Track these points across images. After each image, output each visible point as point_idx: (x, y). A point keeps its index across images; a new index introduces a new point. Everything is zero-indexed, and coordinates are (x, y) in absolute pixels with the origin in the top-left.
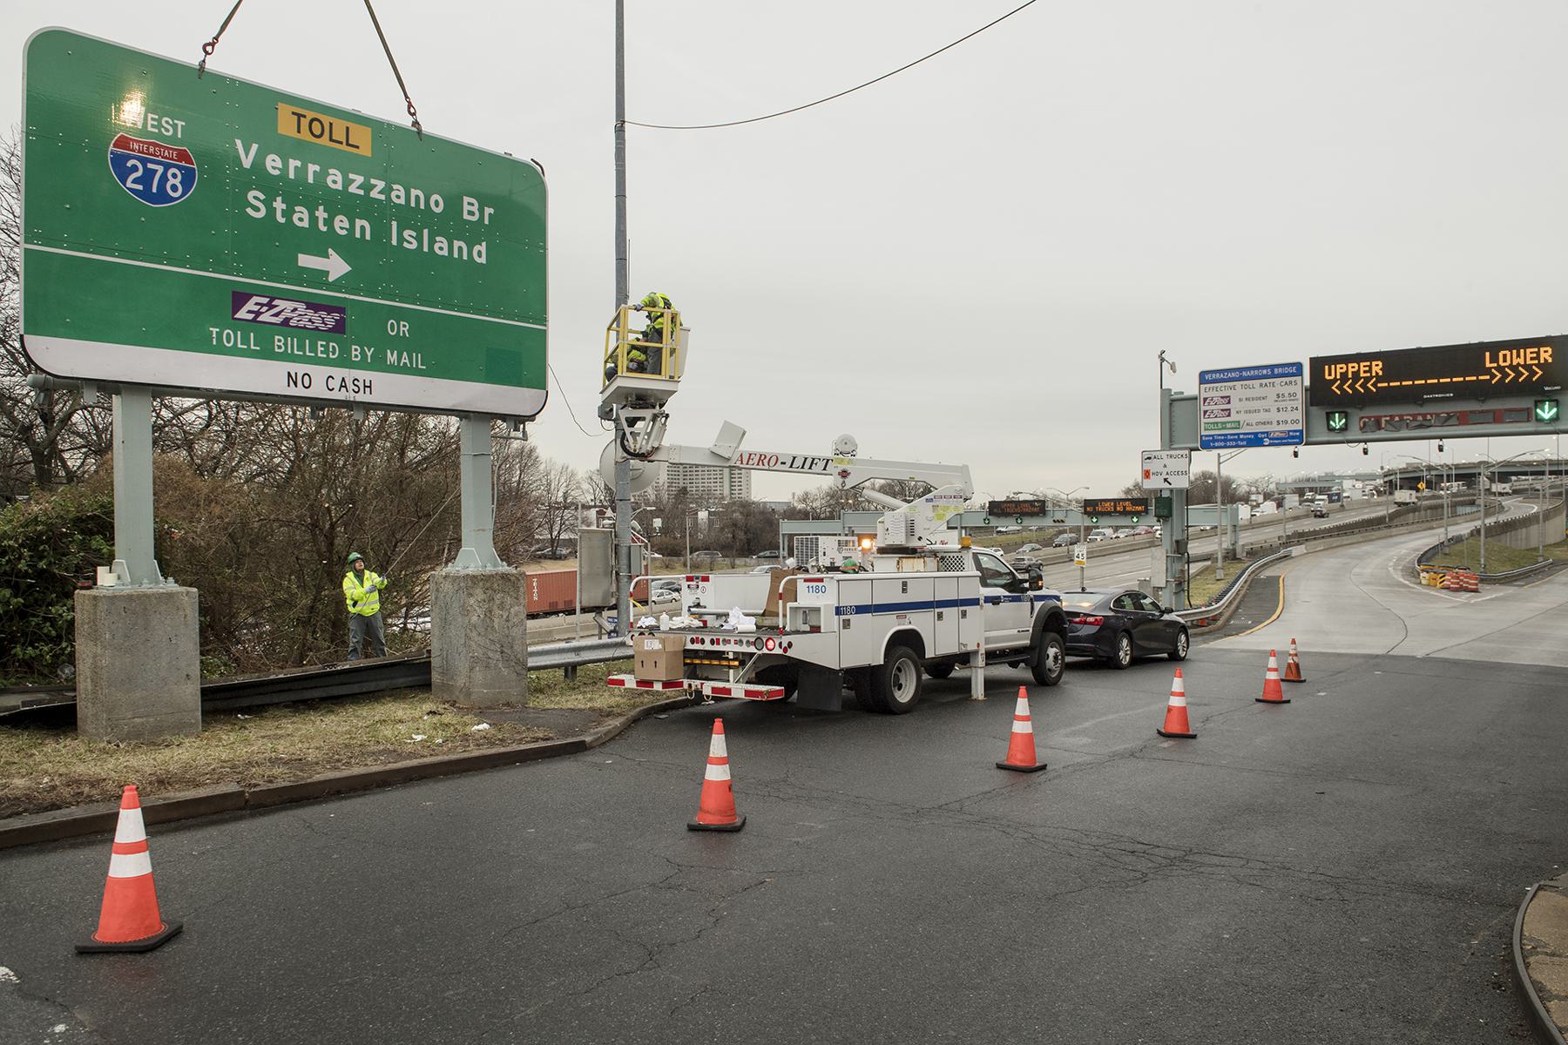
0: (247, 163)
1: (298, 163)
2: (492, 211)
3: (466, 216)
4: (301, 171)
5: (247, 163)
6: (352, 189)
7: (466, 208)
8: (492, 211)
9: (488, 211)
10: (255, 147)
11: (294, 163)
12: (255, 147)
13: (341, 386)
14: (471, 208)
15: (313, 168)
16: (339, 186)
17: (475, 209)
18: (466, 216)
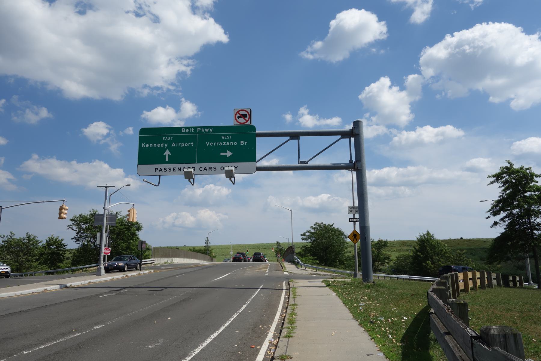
0: (208, 145)
1: (215, 143)
2: (247, 142)
3: (241, 144)
4: (216, 144)
5: (208, 145)
6: (224, 145)
7: (241, 143)
8: (247, 142)
9: (246, 142)
10: (209, 142)
11: (215, 143)
12: (209, 142)
13: (204, 169)
14: (242, 143)
15: (217, 143)
16: (221, 145)
17: (243, 143)
18: (241, 144)
